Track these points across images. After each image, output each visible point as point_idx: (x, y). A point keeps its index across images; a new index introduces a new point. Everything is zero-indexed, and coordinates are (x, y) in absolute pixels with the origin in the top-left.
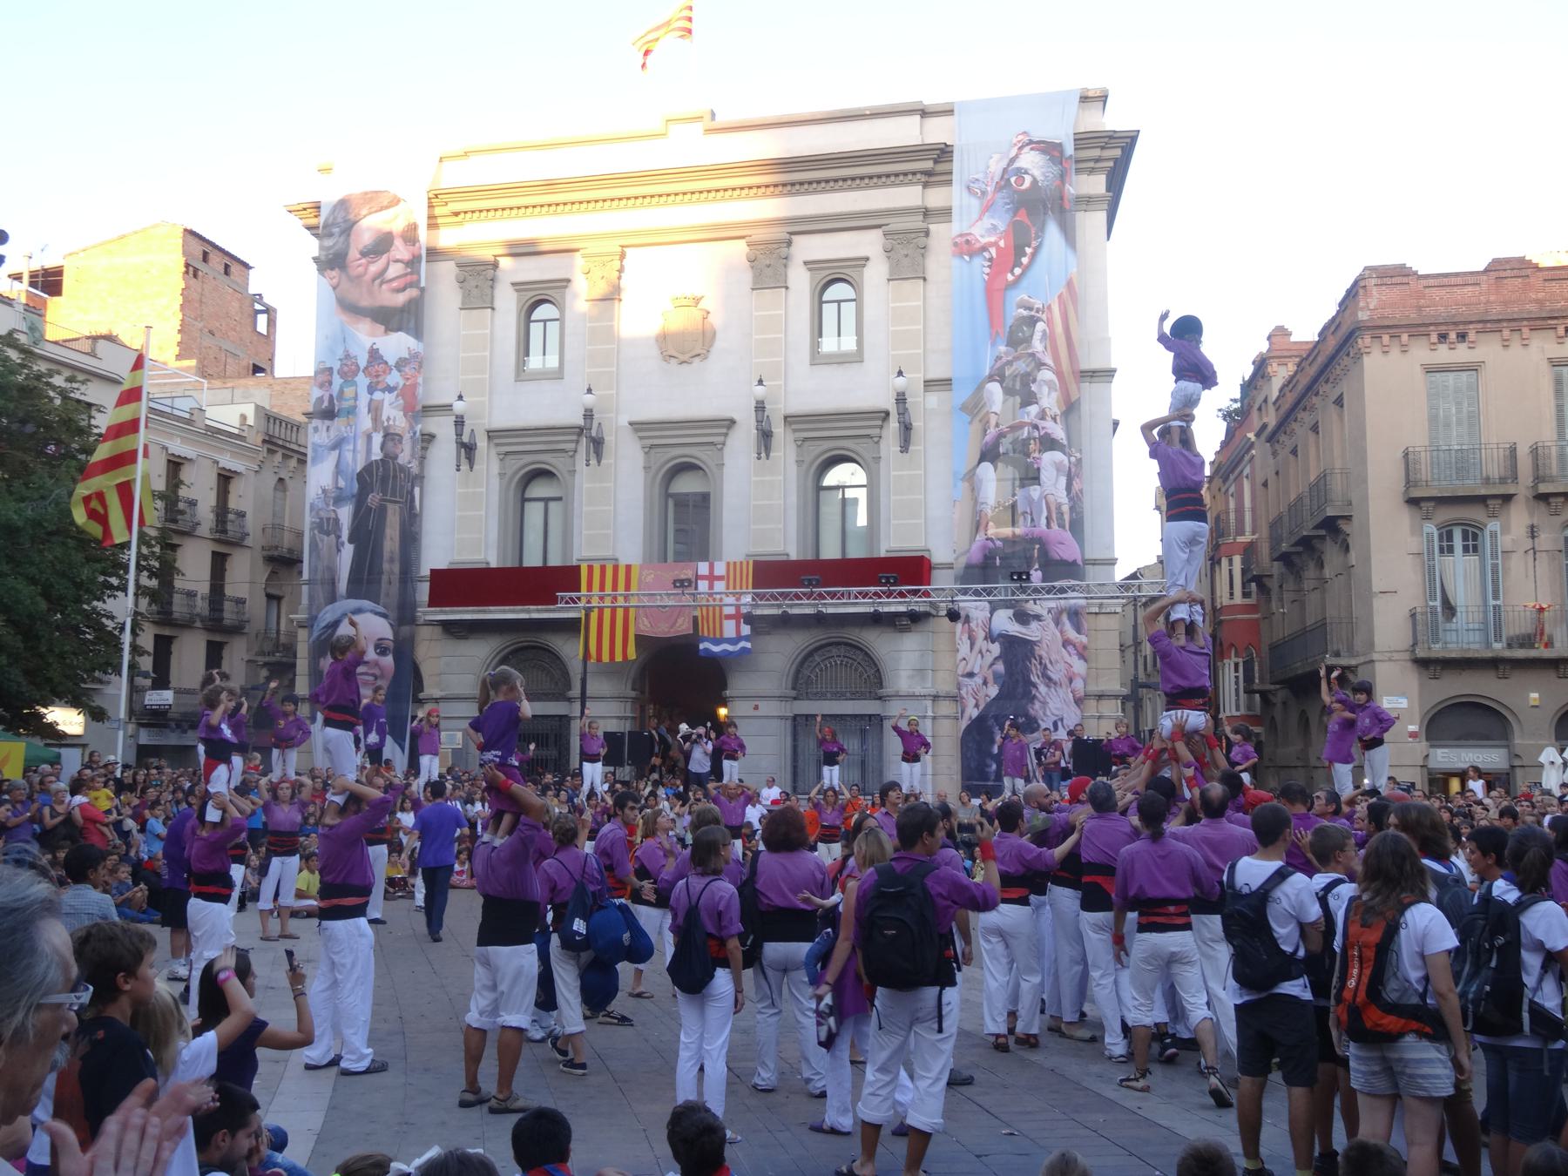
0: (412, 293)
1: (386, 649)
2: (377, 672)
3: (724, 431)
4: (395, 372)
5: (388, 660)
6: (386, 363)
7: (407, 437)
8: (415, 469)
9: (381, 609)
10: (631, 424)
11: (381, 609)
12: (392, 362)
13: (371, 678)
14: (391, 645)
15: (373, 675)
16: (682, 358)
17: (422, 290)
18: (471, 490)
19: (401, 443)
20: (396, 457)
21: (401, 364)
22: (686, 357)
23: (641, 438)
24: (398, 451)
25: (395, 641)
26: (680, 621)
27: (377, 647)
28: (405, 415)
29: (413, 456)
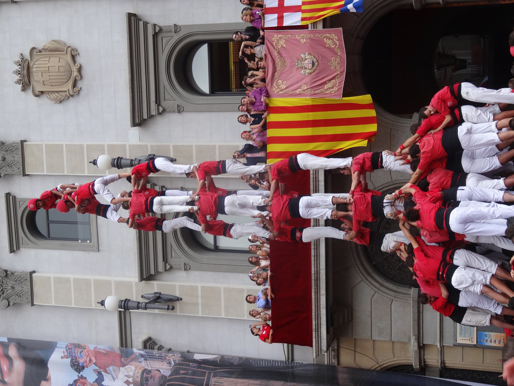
0: (13, 352)
3: (141, 24)
4: (84, 373)
6: (76, 381)
7: (144, 364)
8: (177, 358)
10: (134, 124)
12: (74, 376)
16: (75, 73)
17: (10, 340)
19: (150, 371)
20: (163, 377)
21: (78, 367)
22: (75, 69)
23: (151, 117)
24: (158, 375)
26: (328, 42)
28: (124, 365)
29: (161, 358)
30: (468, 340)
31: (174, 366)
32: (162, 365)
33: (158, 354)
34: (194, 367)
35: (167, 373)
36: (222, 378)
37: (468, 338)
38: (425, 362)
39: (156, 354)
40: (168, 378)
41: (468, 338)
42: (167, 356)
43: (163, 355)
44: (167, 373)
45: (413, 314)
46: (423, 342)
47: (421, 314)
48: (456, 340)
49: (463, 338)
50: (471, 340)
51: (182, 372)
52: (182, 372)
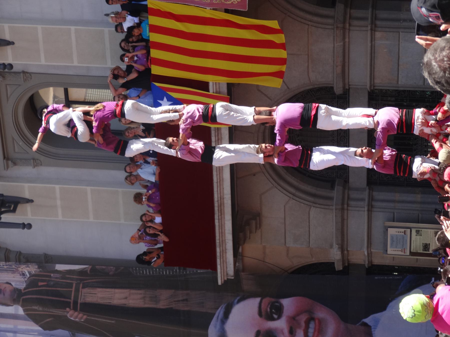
1: (272, 306)
2: (303, 318)
5: (288, 303)
9: (220, 312)
11: (220, 312)
13: (312, 325)
14: (267, 300)
15: (307, 323)
18: (59, 203)
25: (262, 296)
27: (271, 318)
30: (400, 251)
31: (29, 277)
32: (14, 277)
33: (6, 265)
34: (56, 278)
35: (22, 286)
36: (95, 288)
37: (401, 249)
38: (348, 261)
39: (3, 266)
40: (23, 292)
41: (401, 249)
42: (19, 267)
43: (14, 267)
44: (22, 286)
45: (336, 223)
46: (347, 248)
47: (346, 221)
48: (387, 251)
49: (395, 249)
50: (403, 251)
51: (40, 284)
52: (40, 284)
